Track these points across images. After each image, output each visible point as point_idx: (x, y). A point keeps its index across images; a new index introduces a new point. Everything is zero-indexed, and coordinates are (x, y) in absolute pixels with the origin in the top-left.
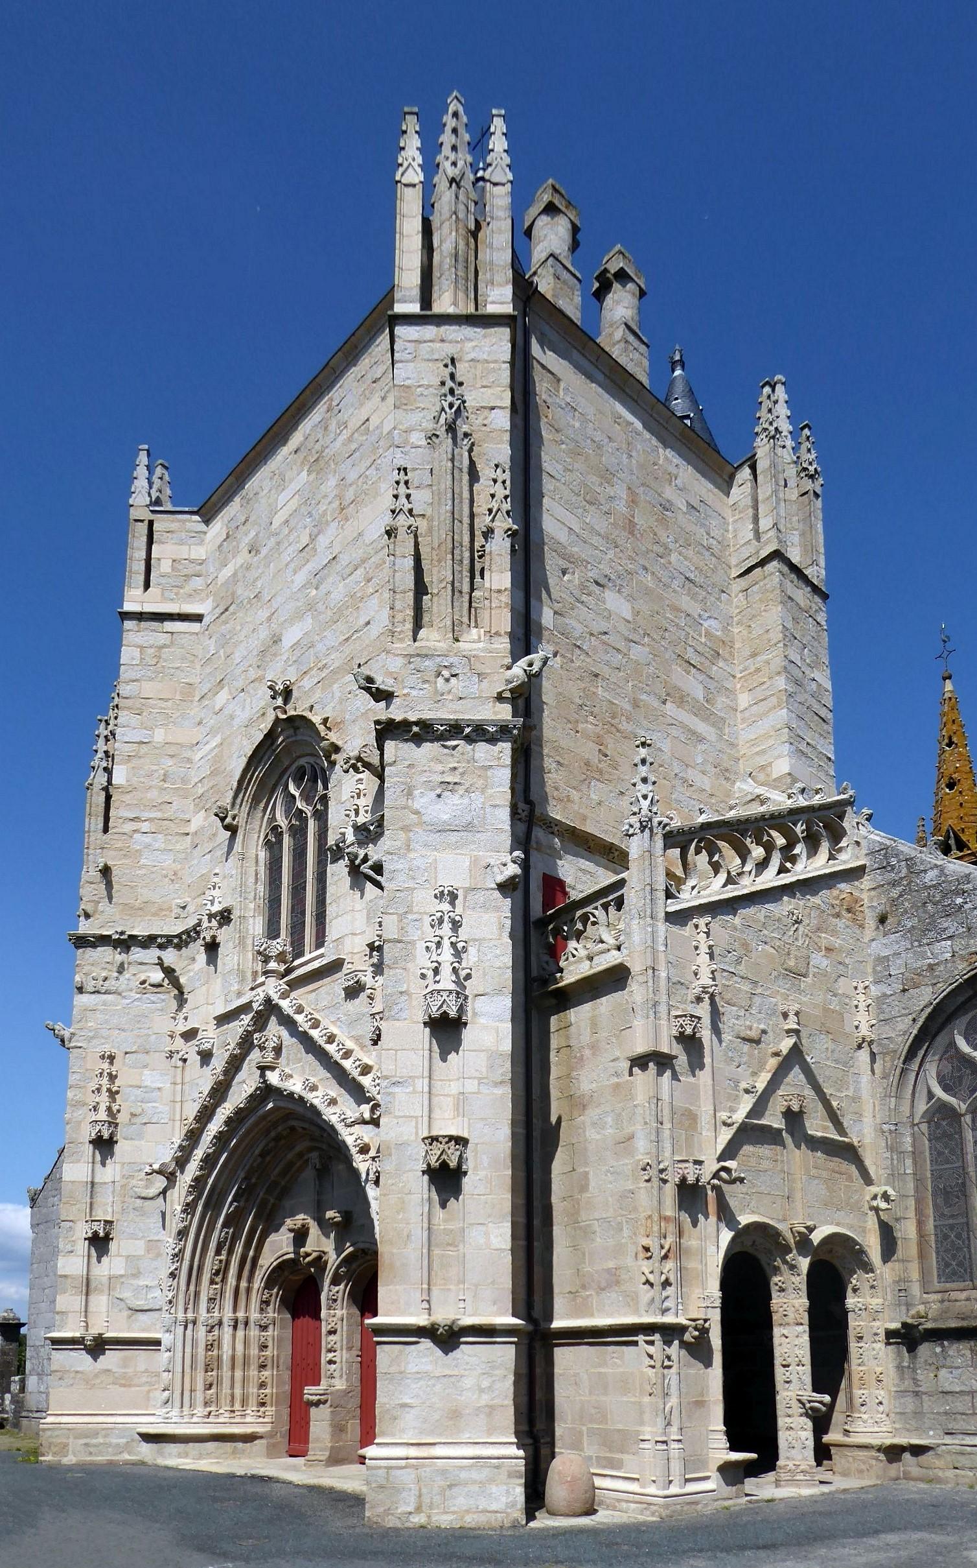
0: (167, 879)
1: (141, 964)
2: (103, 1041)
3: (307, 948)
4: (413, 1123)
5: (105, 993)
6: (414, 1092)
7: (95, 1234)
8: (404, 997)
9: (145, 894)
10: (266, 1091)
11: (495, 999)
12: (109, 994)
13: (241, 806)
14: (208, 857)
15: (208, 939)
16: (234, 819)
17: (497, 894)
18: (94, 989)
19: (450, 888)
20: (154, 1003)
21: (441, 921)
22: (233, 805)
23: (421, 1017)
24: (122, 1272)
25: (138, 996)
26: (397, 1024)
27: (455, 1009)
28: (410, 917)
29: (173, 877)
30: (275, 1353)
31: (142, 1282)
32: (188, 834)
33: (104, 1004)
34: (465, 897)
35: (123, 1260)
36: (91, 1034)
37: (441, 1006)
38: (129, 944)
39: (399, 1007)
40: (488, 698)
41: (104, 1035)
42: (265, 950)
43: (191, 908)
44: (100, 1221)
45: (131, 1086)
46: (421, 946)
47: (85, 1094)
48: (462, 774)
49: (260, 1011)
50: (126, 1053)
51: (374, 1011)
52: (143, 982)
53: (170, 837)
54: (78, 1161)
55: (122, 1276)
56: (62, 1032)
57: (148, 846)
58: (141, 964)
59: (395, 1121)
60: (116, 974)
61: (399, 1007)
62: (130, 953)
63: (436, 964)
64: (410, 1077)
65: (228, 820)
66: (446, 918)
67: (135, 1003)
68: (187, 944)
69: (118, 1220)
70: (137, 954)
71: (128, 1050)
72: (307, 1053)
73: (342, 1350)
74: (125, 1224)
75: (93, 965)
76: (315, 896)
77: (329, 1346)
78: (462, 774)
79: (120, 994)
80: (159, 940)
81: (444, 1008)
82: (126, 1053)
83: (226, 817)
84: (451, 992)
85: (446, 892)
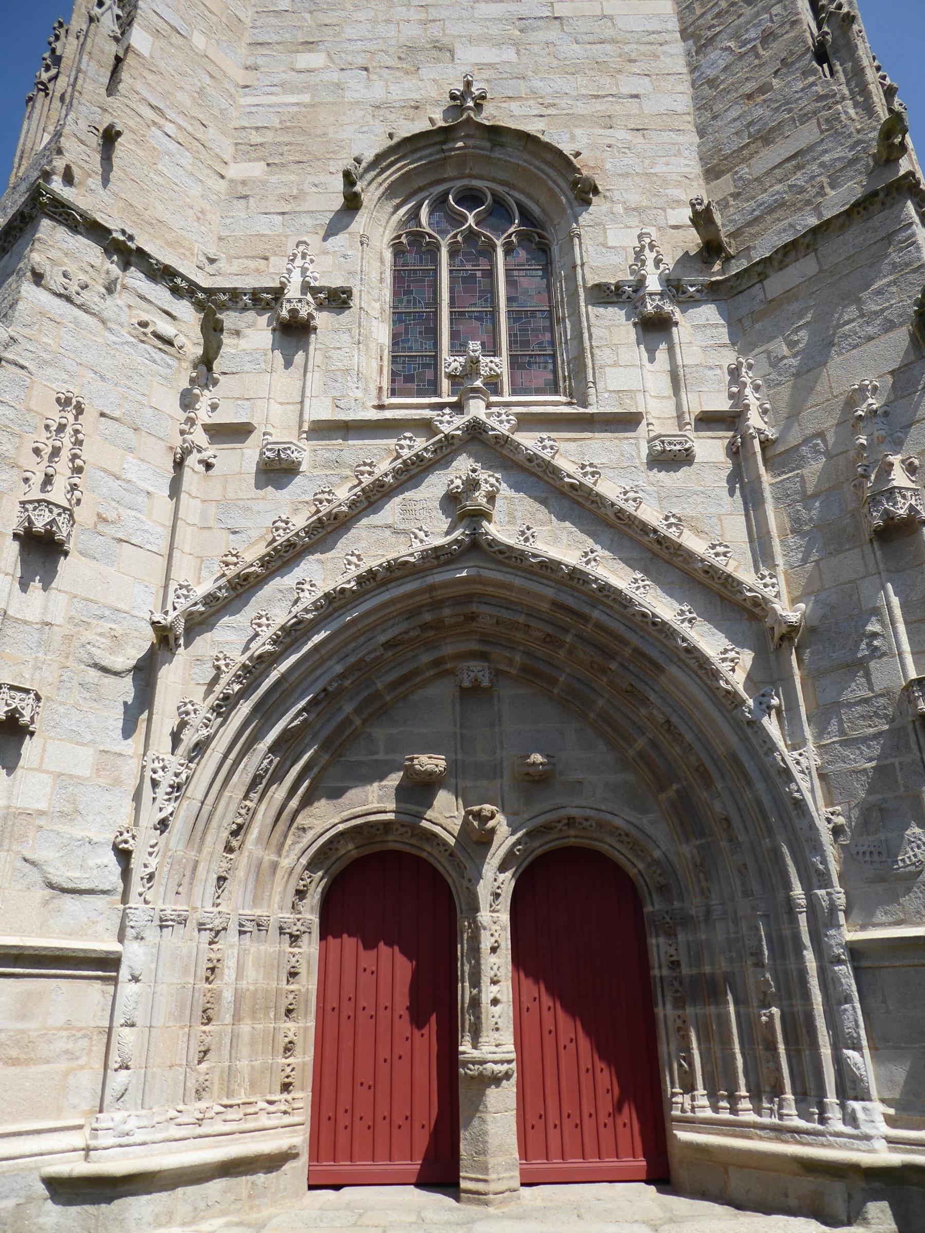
0: (191, 211)
1: (142, 297)
5: (79, 307)
13: (370, 184)
20: (154, 361)
24: (43, 806)
25: (132, 339)
29: (200, 215)
31: (79, 832)
32: (223, 177)
35: (47, 779)
38: (133, 259)
44: (27, 691)
45: (105, 471)
49: (453, 437)
50: (102, 415)
52: (144, 324)
53: (200, 164)
58: (142, 297)
62: (128, 273)
70: (135, 279)
74: (61, 709)
79: (103, 322)
82: (102, 415)
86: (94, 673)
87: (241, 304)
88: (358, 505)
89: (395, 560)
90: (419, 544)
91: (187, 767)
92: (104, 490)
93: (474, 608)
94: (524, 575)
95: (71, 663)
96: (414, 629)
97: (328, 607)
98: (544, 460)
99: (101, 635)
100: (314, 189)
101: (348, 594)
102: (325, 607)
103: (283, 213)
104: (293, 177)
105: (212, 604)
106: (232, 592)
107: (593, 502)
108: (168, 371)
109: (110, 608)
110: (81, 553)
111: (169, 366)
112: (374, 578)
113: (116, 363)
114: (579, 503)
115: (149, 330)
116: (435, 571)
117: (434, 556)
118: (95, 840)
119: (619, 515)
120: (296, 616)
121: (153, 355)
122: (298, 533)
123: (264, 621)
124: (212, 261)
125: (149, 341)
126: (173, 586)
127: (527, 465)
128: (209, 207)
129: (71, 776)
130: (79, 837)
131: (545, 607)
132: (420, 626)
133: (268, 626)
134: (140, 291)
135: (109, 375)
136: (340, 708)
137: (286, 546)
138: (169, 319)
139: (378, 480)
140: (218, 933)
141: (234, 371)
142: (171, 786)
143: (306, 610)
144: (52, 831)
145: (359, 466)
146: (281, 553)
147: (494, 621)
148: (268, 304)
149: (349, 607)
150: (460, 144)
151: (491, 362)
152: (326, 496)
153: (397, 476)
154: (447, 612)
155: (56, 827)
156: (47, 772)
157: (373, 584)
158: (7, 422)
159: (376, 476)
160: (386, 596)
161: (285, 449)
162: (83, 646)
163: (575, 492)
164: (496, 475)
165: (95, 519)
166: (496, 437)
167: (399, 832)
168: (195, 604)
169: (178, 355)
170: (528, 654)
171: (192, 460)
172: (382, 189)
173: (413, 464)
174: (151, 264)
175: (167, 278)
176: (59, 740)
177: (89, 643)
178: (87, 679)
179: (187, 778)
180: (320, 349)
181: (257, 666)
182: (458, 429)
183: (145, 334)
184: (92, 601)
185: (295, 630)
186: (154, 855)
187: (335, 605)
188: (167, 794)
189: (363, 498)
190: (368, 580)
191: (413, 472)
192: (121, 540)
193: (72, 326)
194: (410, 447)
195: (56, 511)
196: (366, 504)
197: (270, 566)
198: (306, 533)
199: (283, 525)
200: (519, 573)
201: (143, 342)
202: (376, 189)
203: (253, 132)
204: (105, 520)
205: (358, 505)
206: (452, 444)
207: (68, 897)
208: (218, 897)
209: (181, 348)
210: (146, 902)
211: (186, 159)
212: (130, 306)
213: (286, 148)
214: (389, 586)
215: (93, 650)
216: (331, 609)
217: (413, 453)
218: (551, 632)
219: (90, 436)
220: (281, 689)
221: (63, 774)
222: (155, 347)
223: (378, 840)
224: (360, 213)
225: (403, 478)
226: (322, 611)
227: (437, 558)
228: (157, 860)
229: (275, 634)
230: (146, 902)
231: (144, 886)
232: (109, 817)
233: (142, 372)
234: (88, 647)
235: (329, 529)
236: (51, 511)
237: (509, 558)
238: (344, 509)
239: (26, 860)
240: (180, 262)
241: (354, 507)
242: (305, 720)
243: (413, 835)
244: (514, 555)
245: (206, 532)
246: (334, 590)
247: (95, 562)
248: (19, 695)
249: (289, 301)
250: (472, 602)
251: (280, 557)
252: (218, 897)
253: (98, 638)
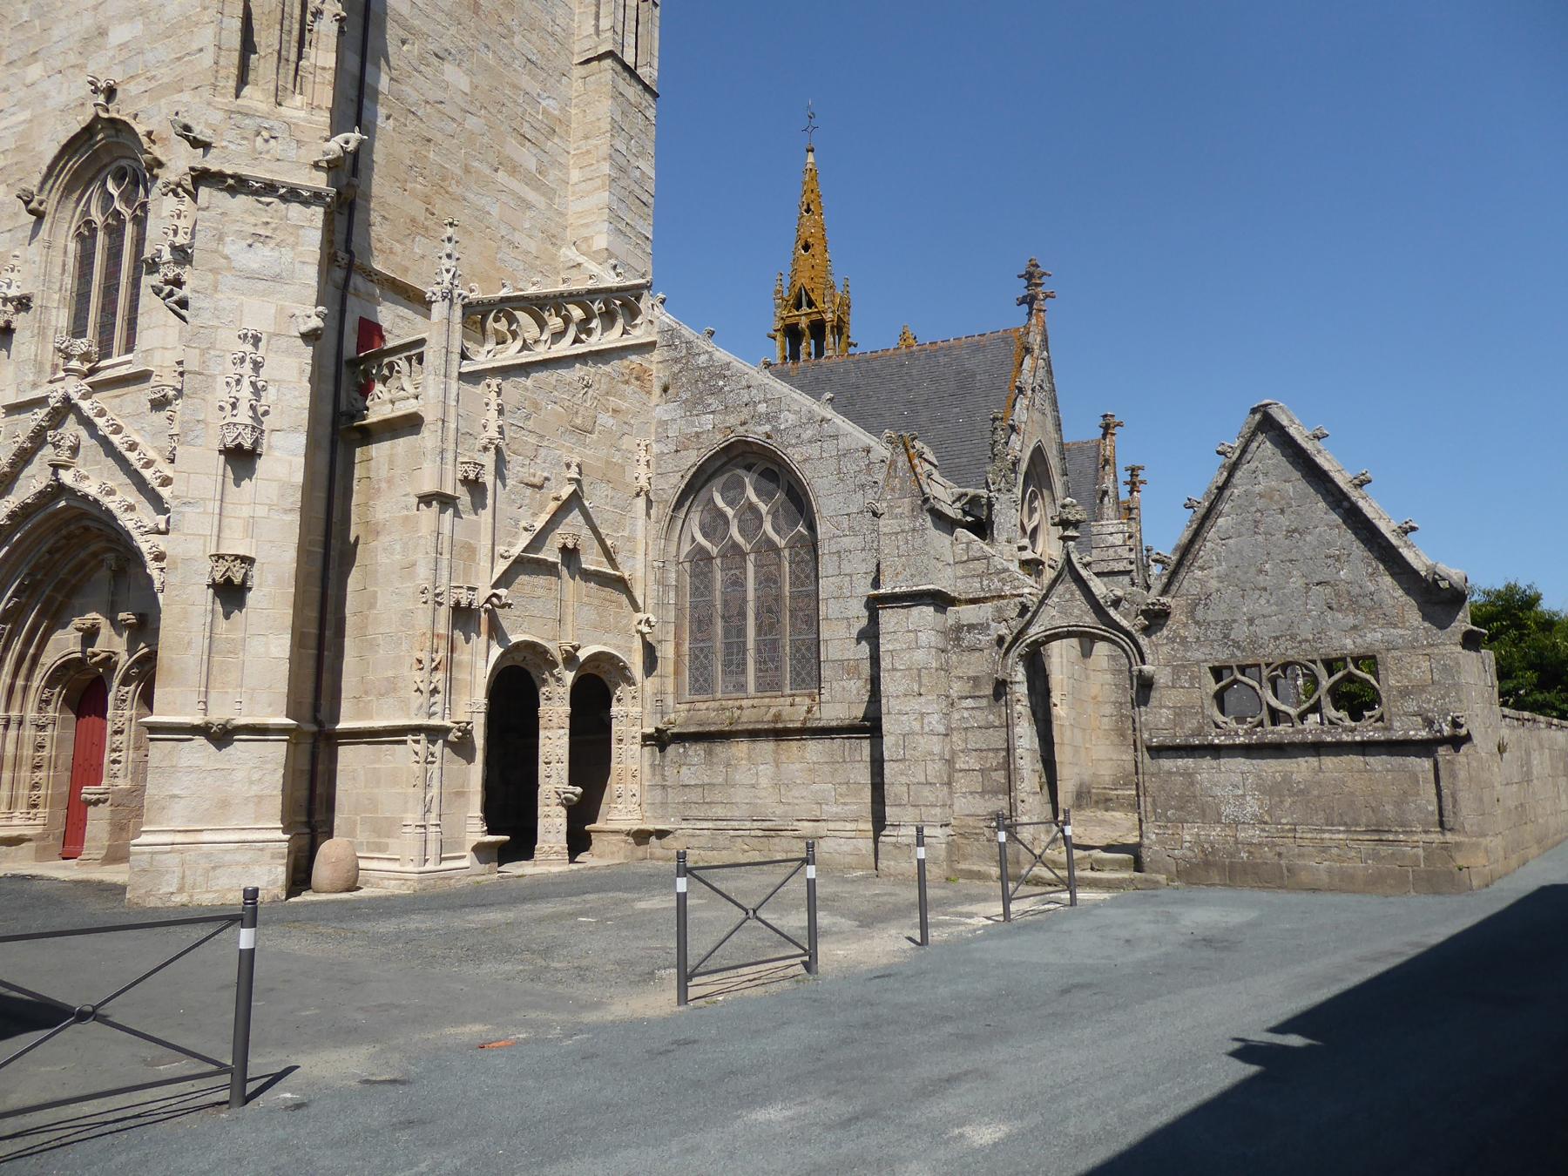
3: (115, 351)
4: (201, 542)
6: (205, 512)
8: (202, 426)
10: (59, 489)
11: (291, 435)
13: (50, 191)
16: (41, 203)
17: (300, 341)
19: (254, 332)
21: (242, 360)
22: (41, 190)
23: (217, 445)
26: (192, 449)
27: (250, 441)
28: (212, 352)
34: (269, 341)
37: (236, 438)
39: (196, 433)
40: (304, 164)
42: (67, 348)
46: (221, 380)
48: (275, 229)
49: (58, 408)
51: (172, 432)
59: (184, 538)
61: (196, 433)
63: (234, 400)
64: (202, 499)
65: (33, 205)
66: (248, 359)
72: (107, 456)
76: (128, 301)
78: (275, 229)
81: (240, 440)
83: (31, 201)
84: (246, 426)
85: (250, 335)
103: (10, 230)
150: (99, 137)
172: (60, 193)
196: (23, 463)
238: (6, 469)
242: (16, 603)
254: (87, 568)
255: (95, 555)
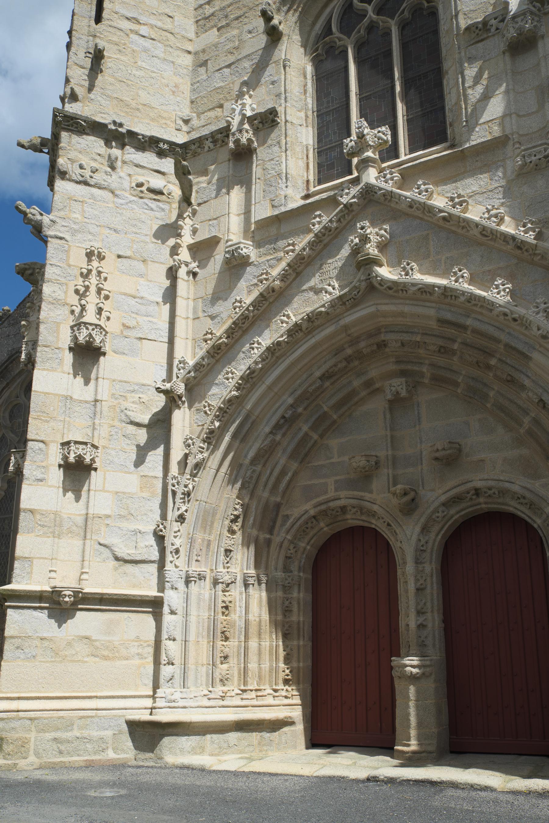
0: (167, 89)
1: (138, 166)
2: (90, 237)
7: (80, 459)
9: (144, 97)
12: (99, 188)
14: (227, 70)
15: (244, 141)
18: (81, 179)
20: (152, 209)
22: (279, 10)
24: (108, 512)
25: (134, 198)
29: (174, 89)
30: (301, 619)
32: (189, 52)
33: (93, 197)
36: (75, 227)
41: (92, 230)
43: (195, 122)
44: (85, 444)
47: (66, 293)
49: (351, 204)
50: (119, 257)
53: (171, 50)
54: (53, 370)
55: (108, 516)
56: (39, 217)
57: (146, 50)
58: (138, 166)
60: (109, 169)
67: (130, 205)
68: (195, 154)
69: (104, 447)
71: (121, 253)
73: (432, 611)
74: (113, 453)
75: (80, 152)
77: (419, 607)
80: (161, 145)
82: (119, 257)
86: (131, 428)
87: (206, 148)
88: (288, 277)
89: (312, 312)
90: (328, 297)
91: (193, 481)
92: (126, 307)
93: (383, 337)
94: (411, 302)
95: (117, 423)
96: (341, 362)
97: (272, 357)
98: (420, 203)
99: (133, 402)
100: (250, 36)
101: (283, 345)
102: (269, 357)
104: (235, 32)
105: (201, 370)
106: (212, 359)
107: (463, 228)
108: (163, 213)
109: (137, 384)
110: (115, 352)
111: (163, 210)
112: (301, 330)
113: (124, 218)
114: (454, 232)
115: (144, 189)
116: (345, 314)
117: (341, 303)
118: (143, 530)
119: (484, 232)
120: (249, 368)
121: (150, 205)
122: (248, 308)
123: (230, 375)
124: (186, 122)
125: (146, 196)
126: (176, 362)
127: (410, 211)
128: (181, 81)
129: (124, 493)
130: (133, 530)
131: (433, 324)
132: (346, 359)
133: (232, 378)
134: (135, 161)
135: (119, 228)
136: (300, 429)
137: (242, 320)
138: (160, 176)
139: (298, 254)
140: (228, 585)
141: (206, 199)
142: (183, 494)
143: (256, 363)
144: (115, 526)
145: (285, 247)
146: (240, 325)
147: (399, 344)
148: (223, 142)
149: (288, 354)
151: (379, 132)
152: (264, 276)
153: (314, 248)
154: (362, 344)
155: (117, 524)
156: (108, 492)
157: (301, 334)
158: (56, 277)
159: (297, 252)
160: (313, 341)
161: (236, 249)
162: (122, 411)
163: (448, 224)
164: (384, 227)
165: (122, 328)
166: (384, 195)
167: (352, 512)
168: (189, 372)
169: (168, 200)
170: (432, 365)
171: (182, 272)
173: (324, 235)
174: (140, 139)
175: (153, 146)
176: (113, 471)
177: (126, 409)
178: (128, 432)
179: (194, 488)
180: (259, 165)
181: (229, 408)
182: (354, 197)
183: (142, 192)
184: (125, 382)
185: (252, 378)
186: (178, 537)
187: (277, 355)
188: (181, 499)
189: (290, 271)
190: (297, 332)
191: (325, 242)
192: (141, 339)
193: (92, 201)
194: (319, 223)
195: (90, 328)
197: (234, 336)
198: (253, 306)
199: (239, 304)
200: (408, 302)
201: (141, 198)
202: (293, 15)
203: (207, 6)
204: (128, 327)
205: (288, 277)
206: (352, 211)
207: (129, 566)
208: (227, 563)
209: (169, 194)
210: (176, 567)
211: (159, 50)
212: (130, 175)
213: (229, 10)
214: (314, 333)
215: (128, 413)
216: (274, 358)
217: (321, 226)
218: (442, 344)
219: (112, 273)
220: (250, 421)
221: (118, 492)
222: (151, 199)
223: (340, 519)
224: (281, 42)
225: (319, 247)
226: (267, 361)
227: (344, 304)
228: (180, 541)
229: (237, 383)
230: (176, 567)
231: (173, 557)
232: (152, 516)
233: (143, 220)
234: (126, 411)
235: (271, 300)
236: (87, 329)
237: (397, 291)
239: (100, 544)
240: (163, 130)
241: (285, 279)
243: (362, 513)
244: (400, 288)
245: (197, 320)
246: (273, 344)
247: (124, 356)
248: (81, 447)
249: (234, 134)
250: (381, 333)
251: (240, 327)
252: (227, 563)
253: (131, 405)
254: (356, 399)
255: (368, 384)
